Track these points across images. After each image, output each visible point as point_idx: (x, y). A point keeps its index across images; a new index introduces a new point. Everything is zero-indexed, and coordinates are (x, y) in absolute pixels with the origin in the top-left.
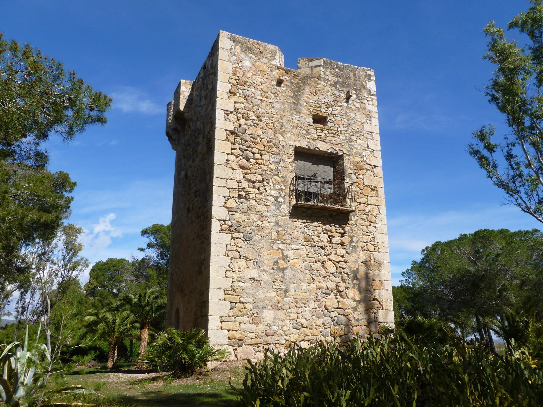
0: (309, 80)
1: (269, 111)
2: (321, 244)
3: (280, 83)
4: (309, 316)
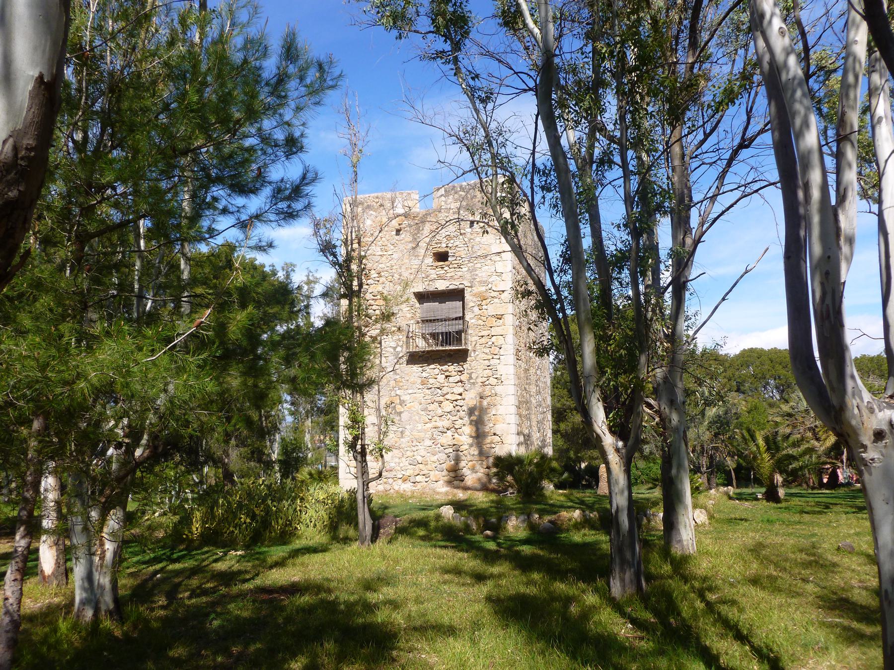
0: (428, 217)
1: (388, 265)
2: (438, 385)
3: (398, 232)
4: (423, 453)
